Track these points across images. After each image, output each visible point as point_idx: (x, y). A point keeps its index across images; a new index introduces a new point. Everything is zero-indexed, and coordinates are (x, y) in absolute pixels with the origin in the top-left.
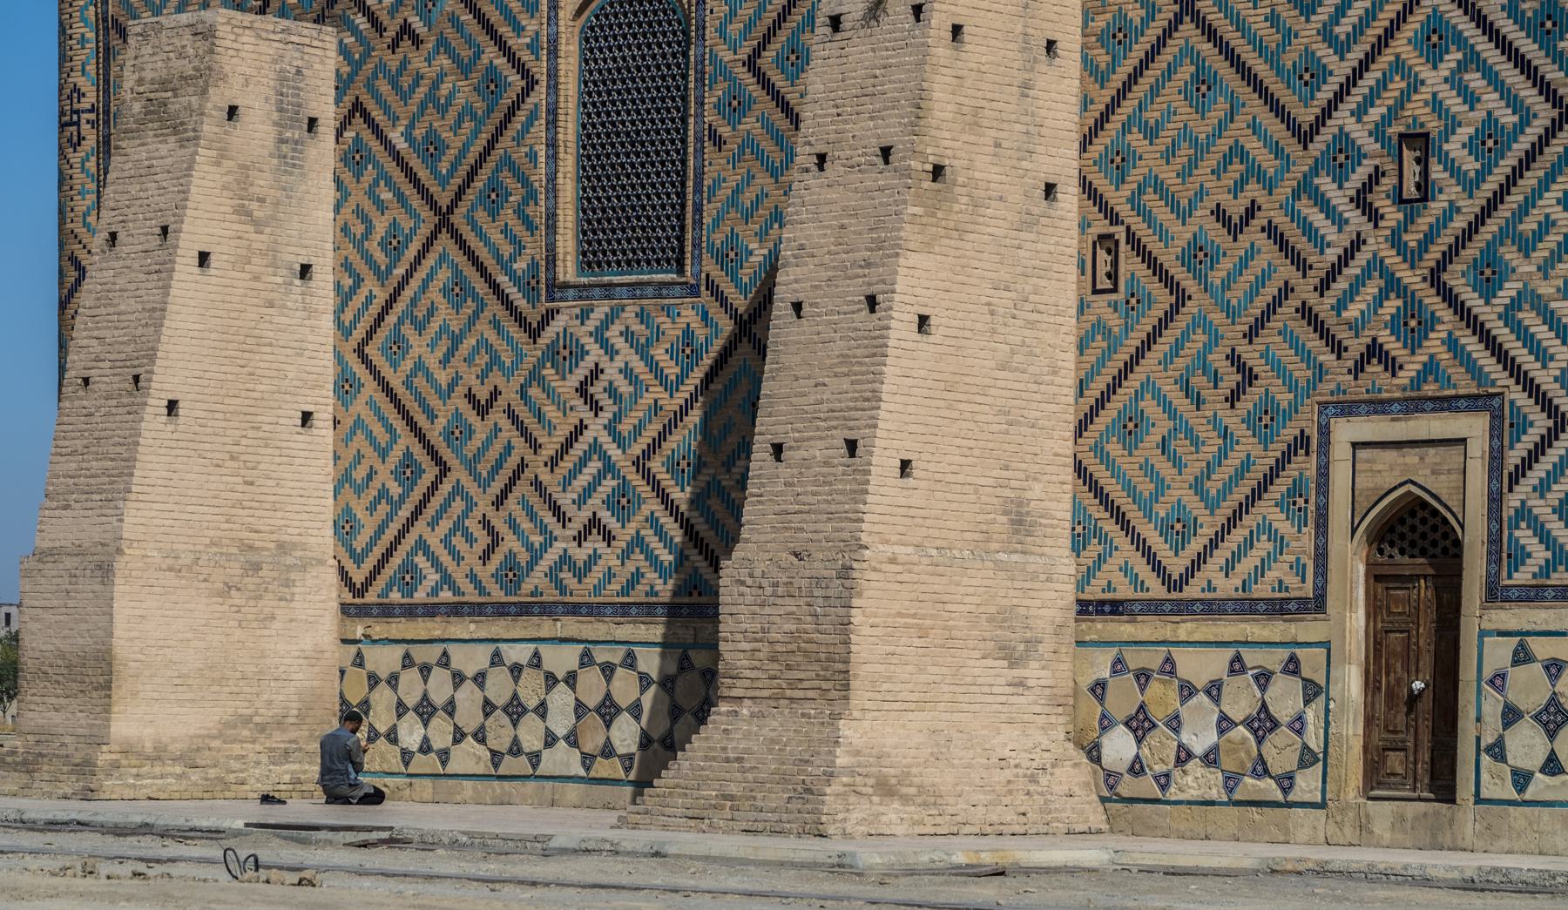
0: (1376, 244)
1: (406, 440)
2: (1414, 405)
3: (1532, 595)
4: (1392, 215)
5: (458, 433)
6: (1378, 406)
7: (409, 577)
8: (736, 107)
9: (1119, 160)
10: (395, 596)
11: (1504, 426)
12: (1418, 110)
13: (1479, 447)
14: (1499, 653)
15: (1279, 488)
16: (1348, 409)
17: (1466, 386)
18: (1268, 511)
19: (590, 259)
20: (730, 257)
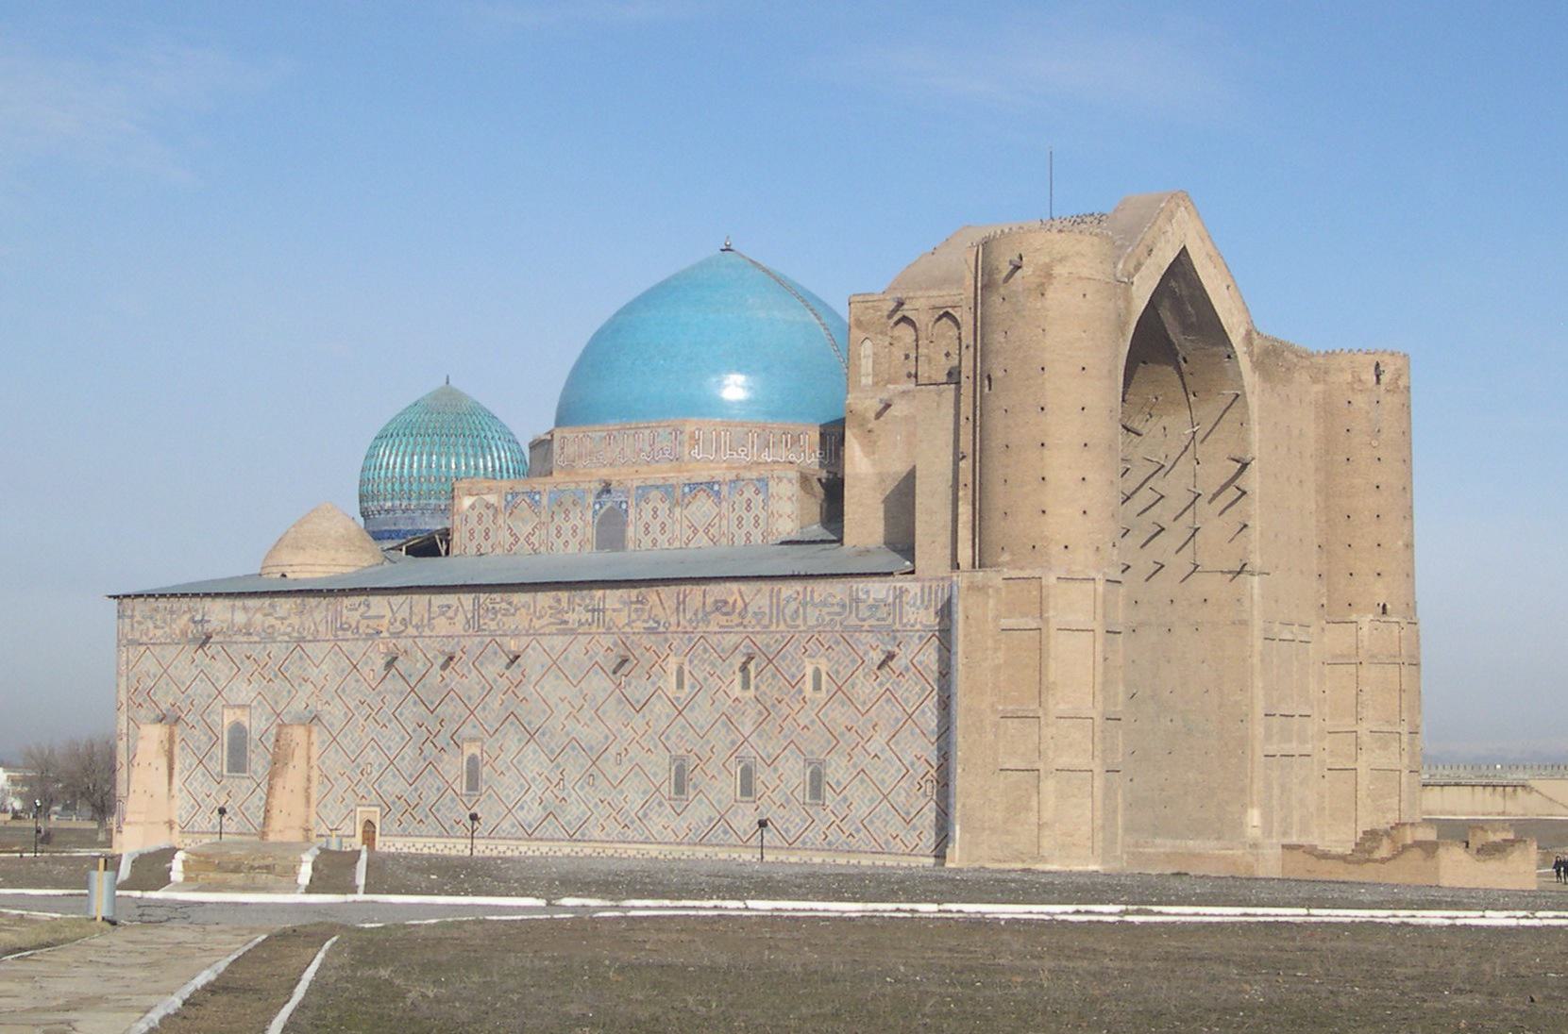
0: (363, 779)
1: (193, 801)
2: (369, 805)
3: (385, 835)
4: (366, 775)
5: (203, 800)
6: (364, 805)
7: (193, 826)
8: (257, 746)
9: (324, 763)
10: (191, 830)
11: (382, 809)
12: (370, 760)
13: (379, 812)
14: (382, 844)
15: (349, 817)
16: (359, 805)
17: (375, 803)
18: (347, 820)
19: (229, 771)
20: (255, 773)
